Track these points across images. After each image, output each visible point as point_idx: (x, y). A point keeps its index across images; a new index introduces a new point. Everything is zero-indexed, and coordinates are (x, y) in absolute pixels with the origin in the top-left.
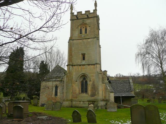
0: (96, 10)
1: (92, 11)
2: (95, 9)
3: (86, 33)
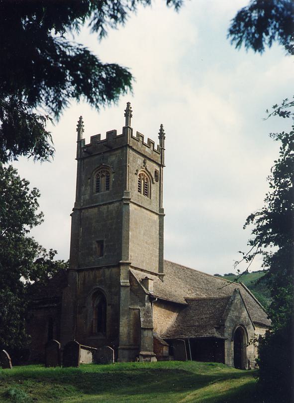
0: (127, 129)
1: (120, 132)
2: (125, 126)
3: (108, 189)
